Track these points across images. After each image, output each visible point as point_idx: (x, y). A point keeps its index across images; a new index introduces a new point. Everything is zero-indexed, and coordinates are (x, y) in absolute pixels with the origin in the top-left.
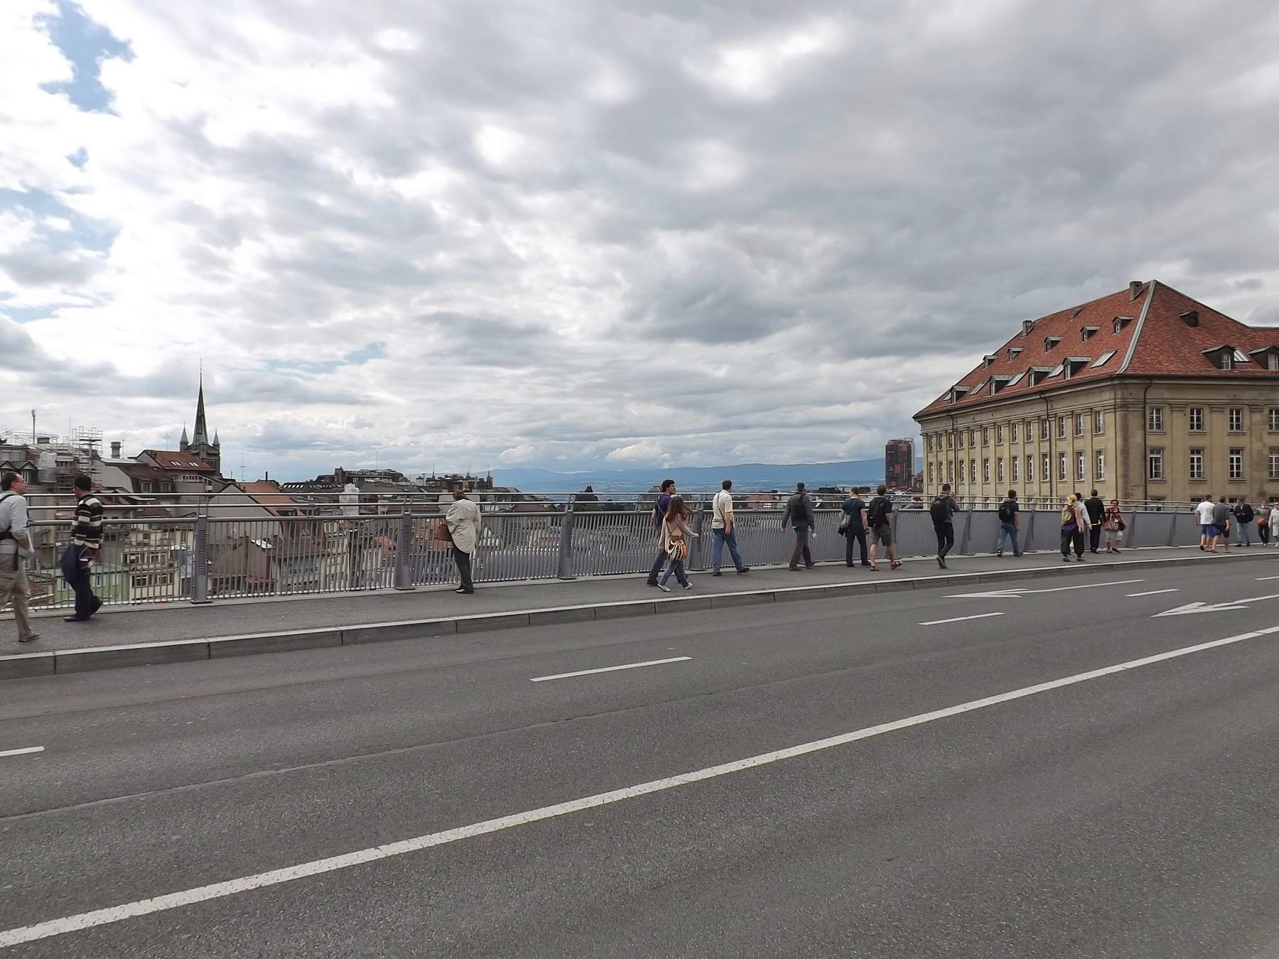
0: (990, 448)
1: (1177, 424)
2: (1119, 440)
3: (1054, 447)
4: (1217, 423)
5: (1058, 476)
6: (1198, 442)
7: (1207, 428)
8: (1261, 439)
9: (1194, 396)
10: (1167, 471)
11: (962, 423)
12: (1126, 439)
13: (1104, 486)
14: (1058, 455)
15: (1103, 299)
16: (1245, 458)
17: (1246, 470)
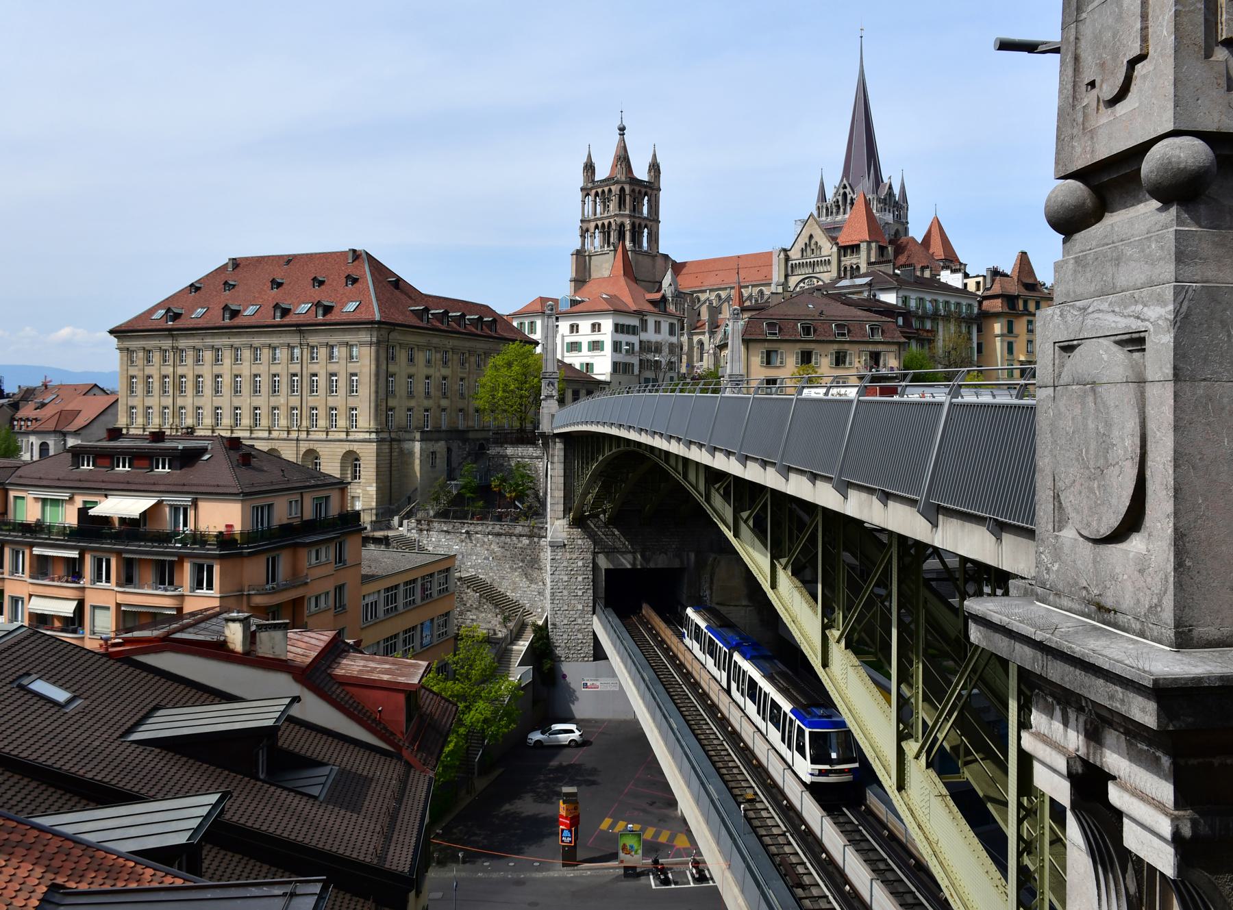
0: (225, 366)
1: (402, 356)
2: (373, 367)
3: (304, 369)
4: (420, 357)
5: (309, 391)
6: (412, 370)
7: (416, 360)
8: (439, 370)
9: (411, 339)
10: (397, 389)
11: (183, 343)
12: (378, 366)
13: (359, 399)
14: (309, 375)
15: (316, 254)
16: (432, 382)
17: (432, 391)
